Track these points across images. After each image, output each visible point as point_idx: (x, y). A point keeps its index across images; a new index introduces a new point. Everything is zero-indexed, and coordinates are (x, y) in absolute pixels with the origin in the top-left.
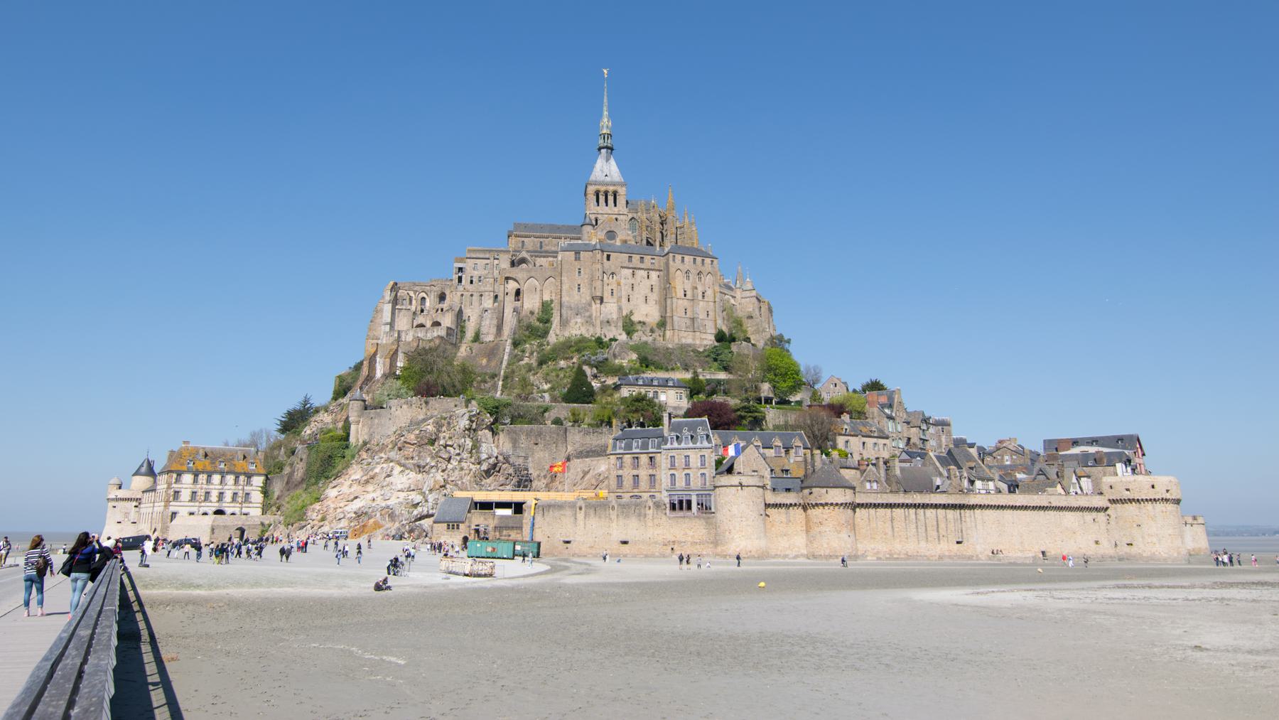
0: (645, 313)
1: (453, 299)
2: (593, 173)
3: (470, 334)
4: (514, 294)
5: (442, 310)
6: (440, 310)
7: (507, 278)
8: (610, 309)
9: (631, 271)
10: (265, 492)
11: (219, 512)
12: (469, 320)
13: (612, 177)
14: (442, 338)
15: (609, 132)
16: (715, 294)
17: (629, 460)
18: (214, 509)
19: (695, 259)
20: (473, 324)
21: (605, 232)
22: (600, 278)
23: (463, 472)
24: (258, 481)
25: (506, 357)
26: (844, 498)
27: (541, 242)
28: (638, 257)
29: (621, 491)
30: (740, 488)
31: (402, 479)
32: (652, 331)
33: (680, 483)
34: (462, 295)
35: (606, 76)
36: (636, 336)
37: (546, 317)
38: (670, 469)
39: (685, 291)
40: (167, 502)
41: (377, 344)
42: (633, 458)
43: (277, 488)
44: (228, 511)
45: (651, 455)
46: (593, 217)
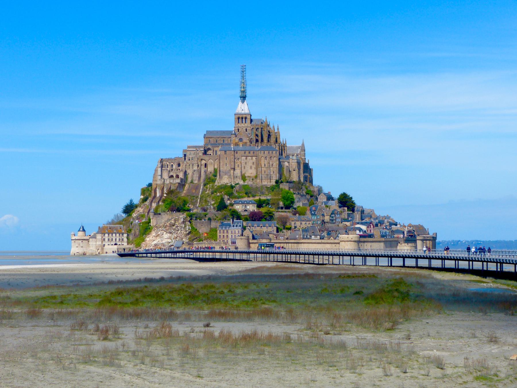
0: (250, 173)
2: (237, 109)
3: (189, 180)
5: (179, 170)
8: (238, 172)
9: (245, 157)
10: (128, 238)
11: (116, 244)
12: (189, 174)
14: (179, 183)
16: (276, 164)
18: (114, 243)
19: (269, 152)
20: (190, 176)
23: (182, 234)
24: (125, 235)
25: (201, 190)
28: (248, 152)
31: (166, 235)
32: (253, 180)
33: (233, 237)
34: (186, 165)
36: (246, 181)
37: (215, 174)
40: (102, 241)
43: (131, 238)
44: (118, 244)
46: (237, 128)
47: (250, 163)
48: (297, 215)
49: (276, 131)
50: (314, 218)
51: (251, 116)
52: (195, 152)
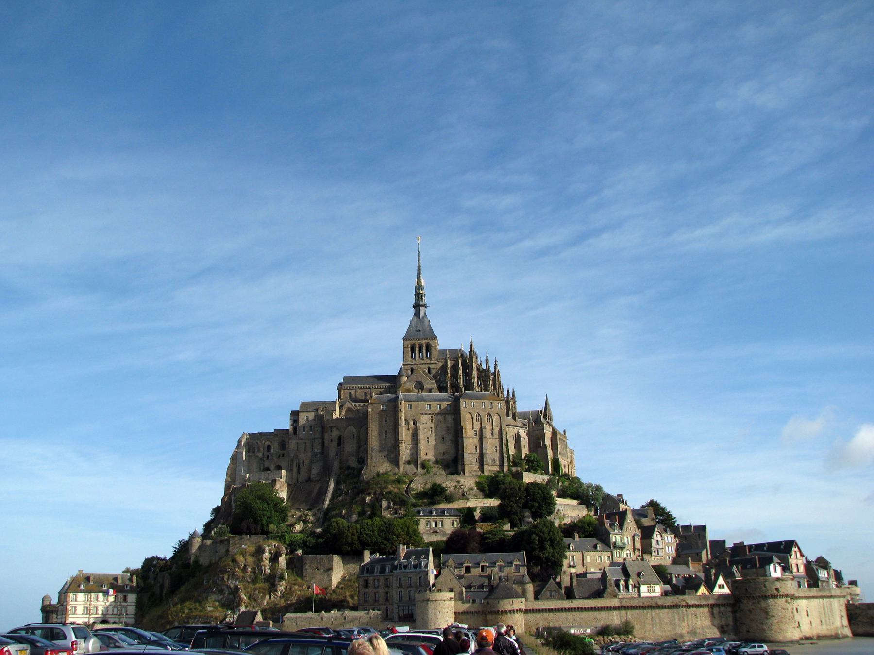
0: (441, 451)
4: (337, 441)
6: (281, 455)
7: (331, 427)
9: (430, 416)
17: (372, 581)
27: (365, 392)
33: (406, 599)
38: (398, 588)
45: (386, 577)
46: (409, 367)
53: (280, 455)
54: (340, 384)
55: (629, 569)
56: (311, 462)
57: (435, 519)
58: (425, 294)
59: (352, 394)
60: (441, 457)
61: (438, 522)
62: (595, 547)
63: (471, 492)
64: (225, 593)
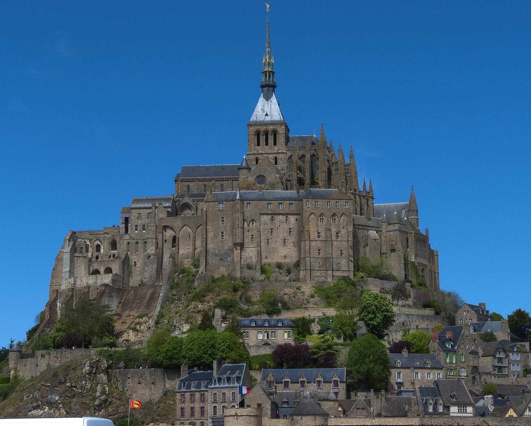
1: (122, 247)
5: (114, 255)
6: (112, 256)
9: (270, 216)
13: (272, 116)
14: (106, 285)
15: (270, 70)
21: (255, 177)
22: (240, 226)
26: (314, 422)
28: (276, 203)
29: (183, 419)
30: (236, 417)
35: (268, 11)
38: (213, 403)
39: (319, 233)
41: (57, 290)
42: (191, 394)
45: (201, 393)
47: (282, 233)
48: (405, 353)
49: (347, 161)
50: (451, 360)
51: (287, 130)
52: (150, 211)
53: (110, 256)
54: (178, 175)
55: (442, 388)
56: (145, 264)
57: (268, 330)
58: (273, 73)
59: (190, 186)
60: (282, 261)
61: (270, 333)
62: (425, 363)
63: (312, 299)
64: (45, 409)
